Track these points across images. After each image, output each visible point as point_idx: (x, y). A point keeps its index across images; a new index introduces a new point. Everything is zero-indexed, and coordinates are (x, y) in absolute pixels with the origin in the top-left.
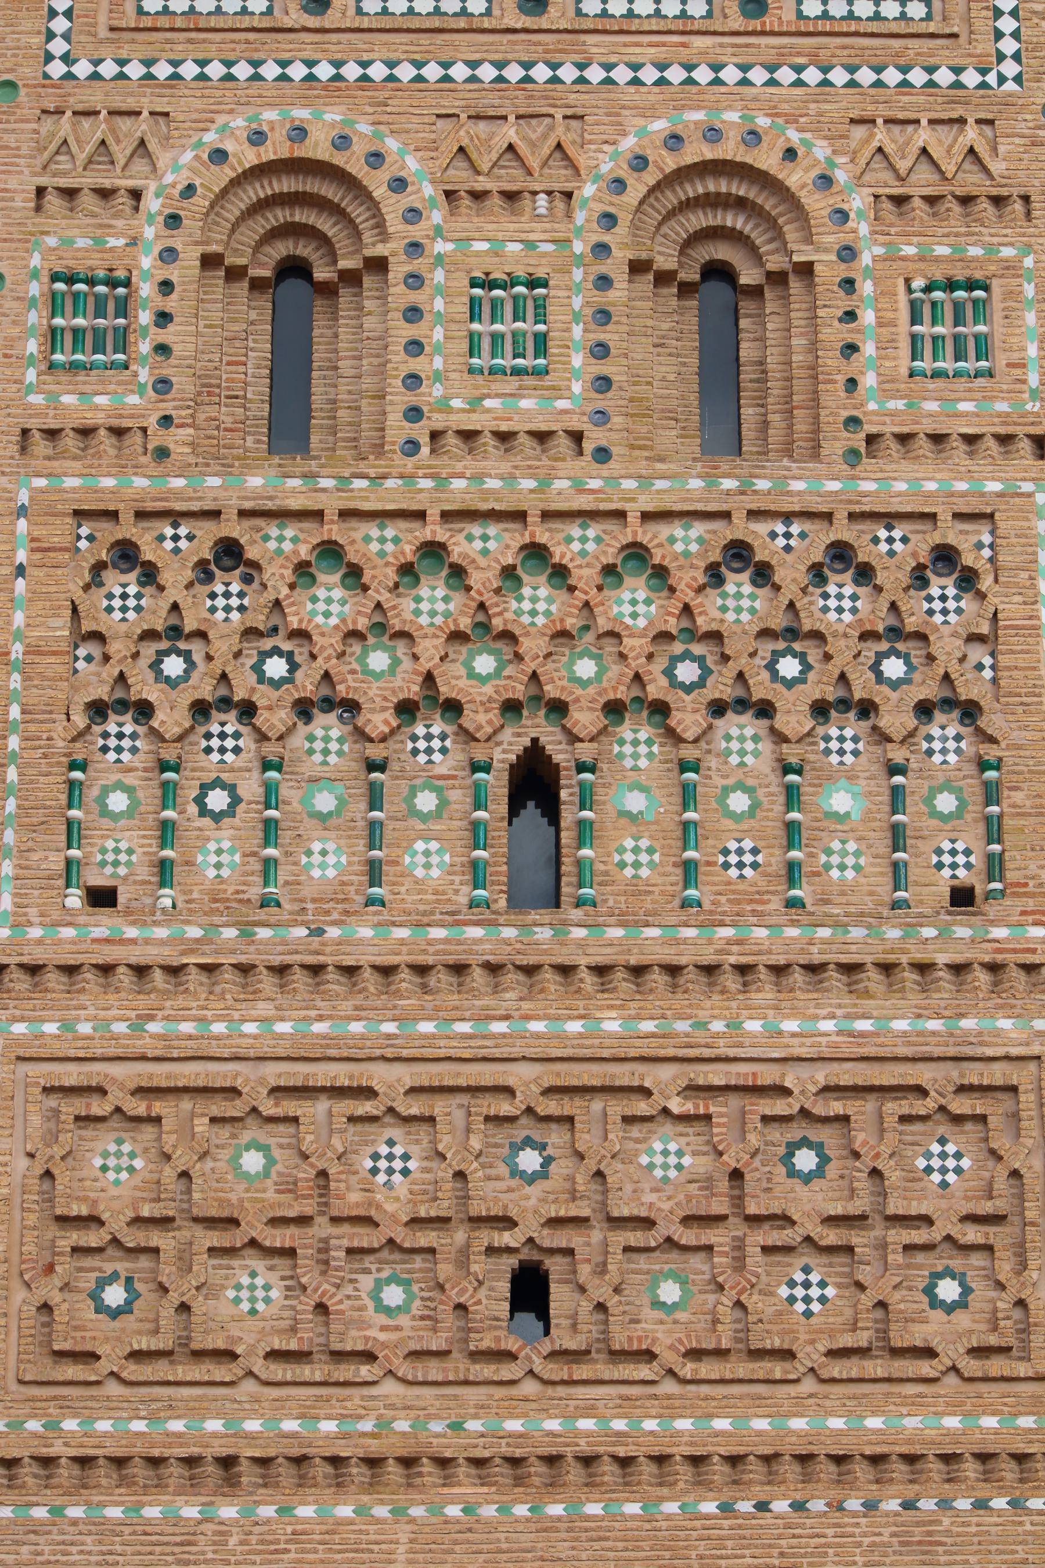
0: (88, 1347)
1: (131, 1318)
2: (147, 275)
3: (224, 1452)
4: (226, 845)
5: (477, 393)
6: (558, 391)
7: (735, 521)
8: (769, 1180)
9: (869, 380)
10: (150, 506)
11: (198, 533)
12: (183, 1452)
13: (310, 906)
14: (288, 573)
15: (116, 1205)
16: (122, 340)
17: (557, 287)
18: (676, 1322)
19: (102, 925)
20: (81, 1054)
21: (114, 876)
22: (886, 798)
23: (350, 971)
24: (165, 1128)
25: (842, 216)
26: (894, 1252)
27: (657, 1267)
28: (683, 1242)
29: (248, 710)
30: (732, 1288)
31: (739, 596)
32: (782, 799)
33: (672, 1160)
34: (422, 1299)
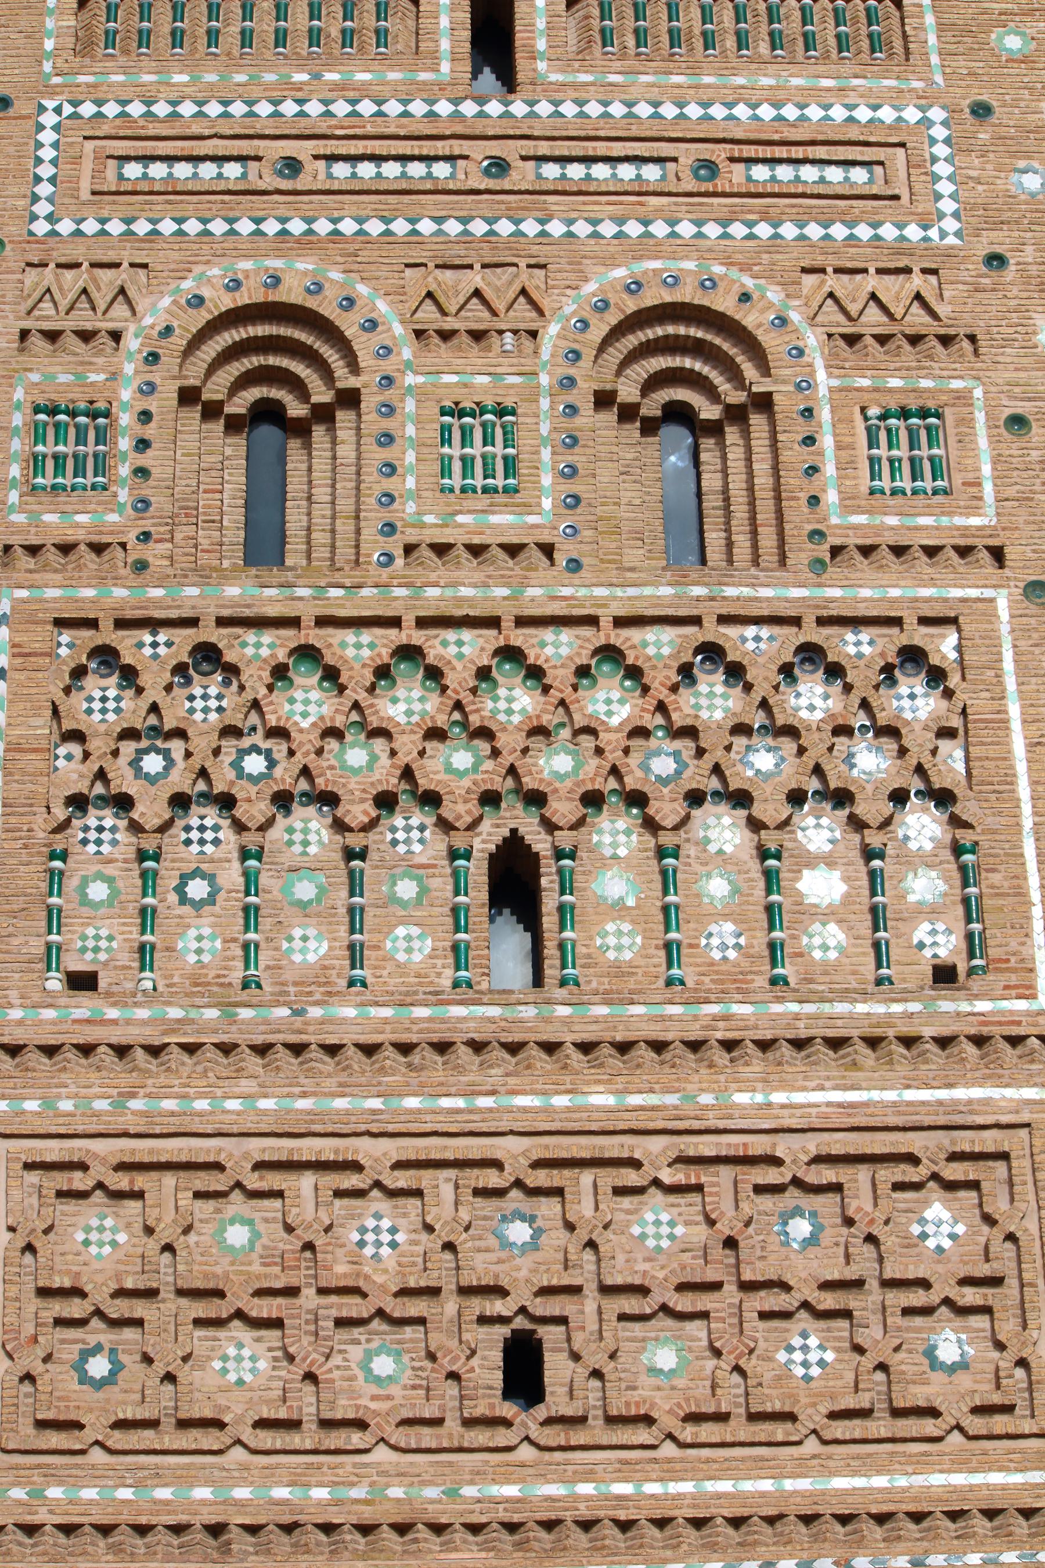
0: (72, 1416)
1: (116, 1389)
2: (125, 407)
3: (213, 1519)
4: (206, 931)
5: (450, 509)
6: (530, 507)
7: (705, 624)
8: (763, 1248)
9: (832, 497)
10: (129, 614)
11: (177, 640)
12: (172, 1520)
13: (292, 989)
14: (266, 675)
15: (99, 1278)
16: (101, 465)
17: (526, 415)
18: (673, 1388)
19: (83, 1006)
20: (62, 1130)
21: (94, 961)
22: (865, 882)
23: (332, 1050)
24: (148, 1202)
26: (893, 1314)
27: (653, 1335)
28: (679, 1308)
29: (226, 802)
30: (730, 1353)
31: (711, 695)
32: (762, 884)
33: (665, 1230)
34: (413, 1368)
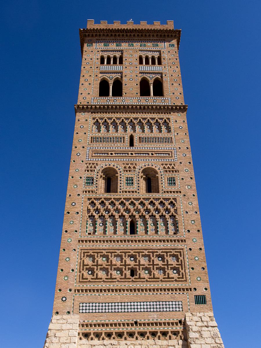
15: (90, 264)
16: (93, 183)
19: (90, 236)
25: (161, 172)
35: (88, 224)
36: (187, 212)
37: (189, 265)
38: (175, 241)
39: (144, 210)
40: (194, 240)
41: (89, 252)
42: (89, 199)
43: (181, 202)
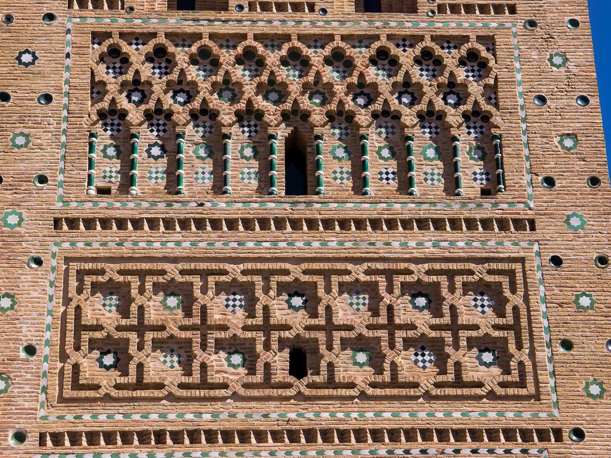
15: (109, 321)
19: (104, 202)
35: (98, 148)
36: (542, 99)
37: (549, 330)
38: (486, 224)
39: (350, 87)
40: (575, 222)
41: (102, 272)
42: (98, 37)
43: (516, 53)
